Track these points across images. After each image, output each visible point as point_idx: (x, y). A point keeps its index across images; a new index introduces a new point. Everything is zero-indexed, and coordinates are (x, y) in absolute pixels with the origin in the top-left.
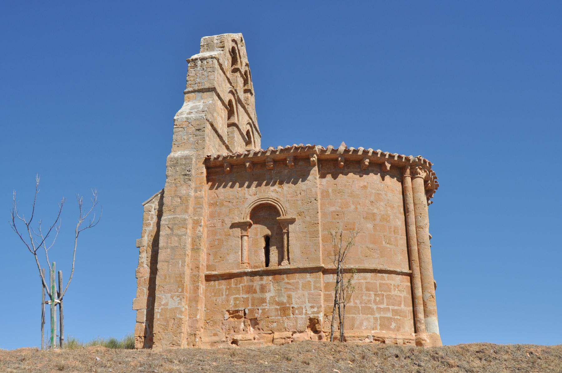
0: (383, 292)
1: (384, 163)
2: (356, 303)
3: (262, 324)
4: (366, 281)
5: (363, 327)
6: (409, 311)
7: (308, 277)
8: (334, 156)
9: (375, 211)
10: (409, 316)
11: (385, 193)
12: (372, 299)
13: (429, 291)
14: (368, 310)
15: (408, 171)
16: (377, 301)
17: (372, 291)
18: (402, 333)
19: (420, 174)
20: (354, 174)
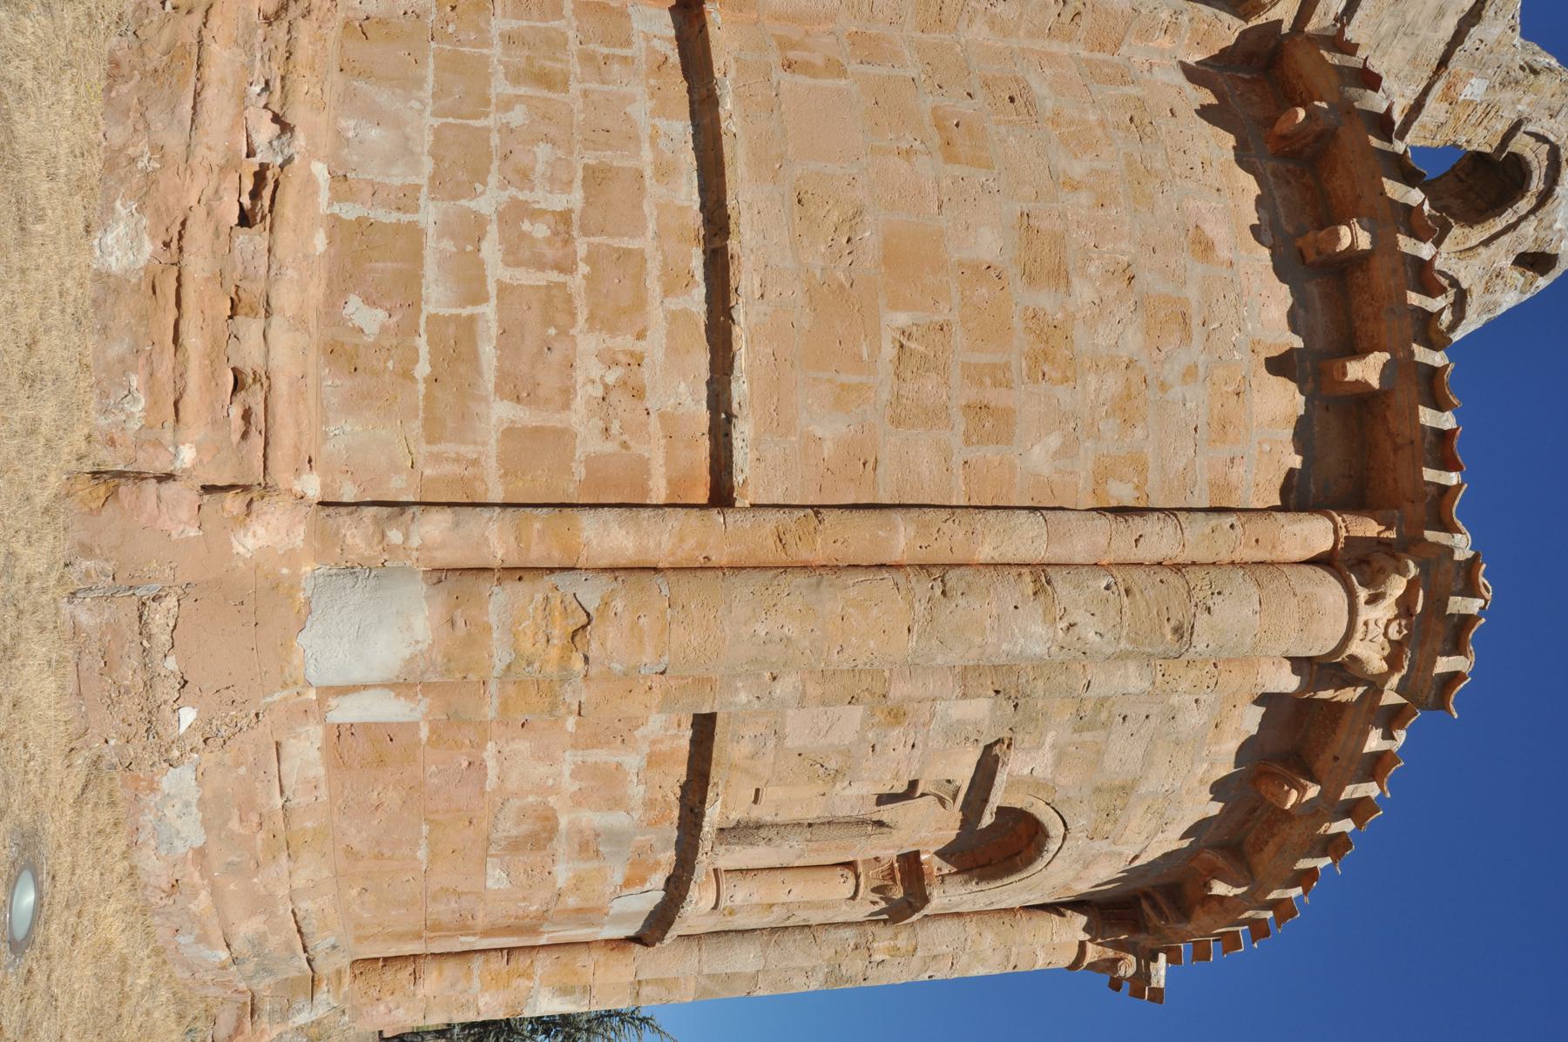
0: (583, 269)
2: (507, 105)
4: (648, 172)
5: (352, 123)
6: (475, 463)
9: (1083, 292)
10: (436, 458)
11: (1201, 370)
12: (539, 194)
13: (619, 604)
15: (1369, 528)
16: (526, 226)
17: (588, 202)
18: (310, 381)
19: (1373, 600)
20: (1260, 202)
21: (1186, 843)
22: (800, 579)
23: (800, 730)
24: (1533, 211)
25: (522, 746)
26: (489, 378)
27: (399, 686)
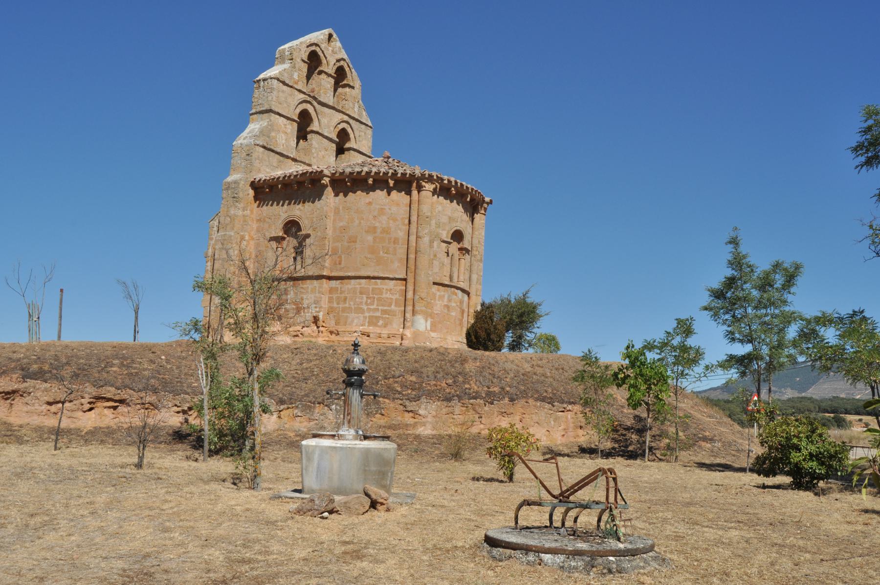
1: (388, 181)
2: (350, 305)
3: (284, 320)
8: (342, 177)
9: (377, 224)
14: (359, 310)
15: (415, 184)
17: (365, 294)
19: (425, 187)
20: (362, 192)
21: (461, 205)
22: (417, 271)
23: (436, 270)
24: (319, 47)
25: (435, 308)
26: (389, 308)
27: (426, 321)
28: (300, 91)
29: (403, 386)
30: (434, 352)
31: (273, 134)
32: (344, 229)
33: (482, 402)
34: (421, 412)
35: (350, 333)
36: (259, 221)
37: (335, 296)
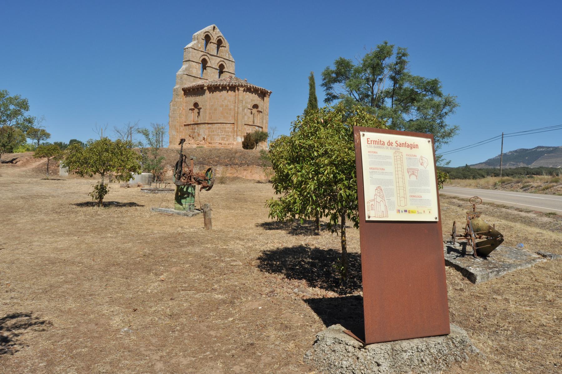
7: (203, 125)
9: (224, 104)
14: (218, 135)
15: (236, 88)
27: (242, 139)
28: (201, 51)
29: (213, 161)
30: (228, 150)
31: (191, 69)
32: (213, 105)
33: (238, 166)
34: (217, 170)
35: (215, 143)
36: (186, 103)
37: (210, 130)
